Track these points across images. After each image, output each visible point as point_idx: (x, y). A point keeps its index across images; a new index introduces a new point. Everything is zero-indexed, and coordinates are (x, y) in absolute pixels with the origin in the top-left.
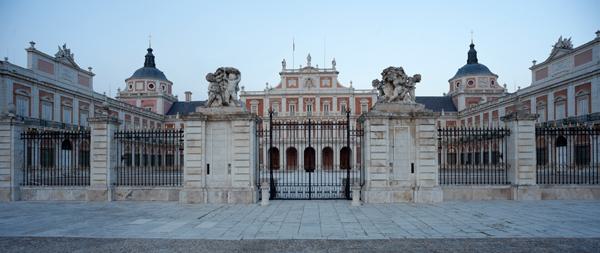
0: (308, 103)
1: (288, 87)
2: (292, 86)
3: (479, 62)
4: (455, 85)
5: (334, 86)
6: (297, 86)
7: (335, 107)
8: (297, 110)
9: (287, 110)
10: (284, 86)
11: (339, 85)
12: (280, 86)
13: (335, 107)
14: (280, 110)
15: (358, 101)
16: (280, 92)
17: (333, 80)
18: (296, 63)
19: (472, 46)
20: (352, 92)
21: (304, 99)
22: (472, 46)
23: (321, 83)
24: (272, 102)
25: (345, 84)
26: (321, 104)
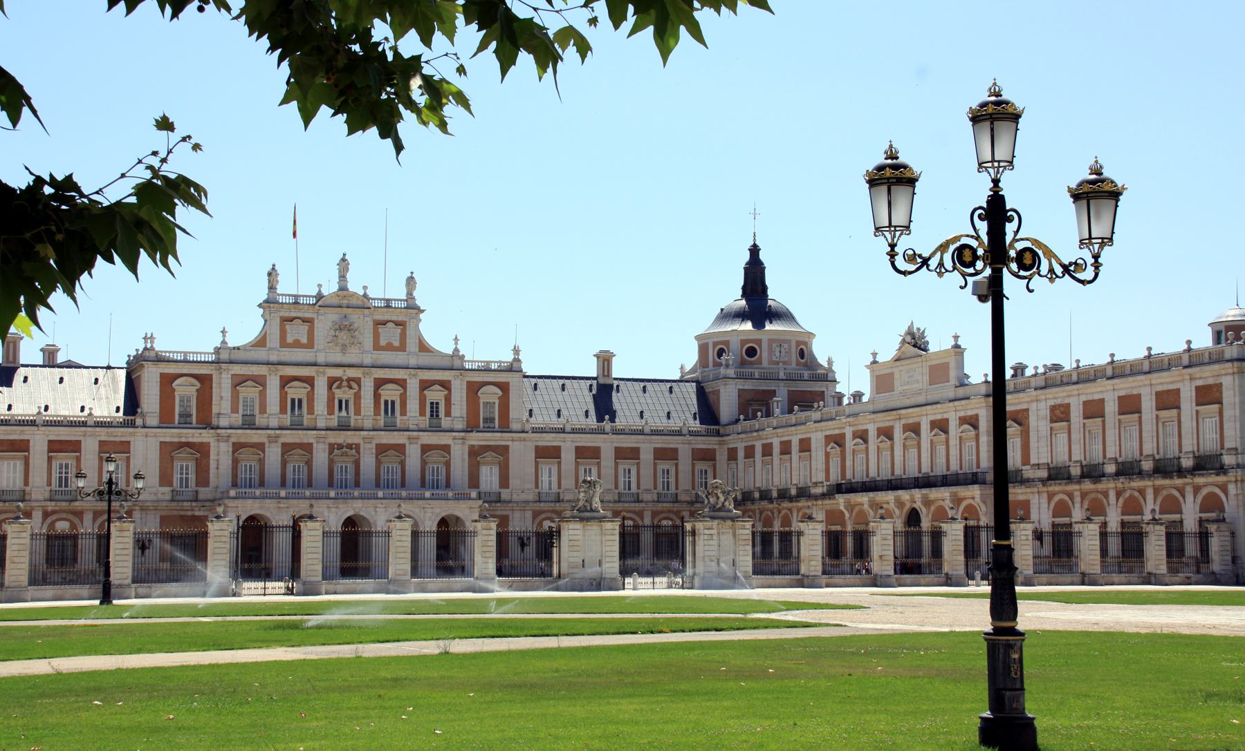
0: (339, 394)
1: (284, 344)
2: (297, 344)
3: (771, 293)
4: (712, 354)
5: (412, 346)
6: (310, 345)
7: (413, 405)
8: (311, 410)
9: (283, 410)
10: (273, 340)
11: (424, 347)
12: (261, 342)
13: (413, 405)
14: (263, 410)
15: (474, 389)
16: (261, 354)
17: (410, 332)
18: (308, 278)
19: (755, 250)
20: (457, 363)
21: (332, 382)
22: (755, 250)
23: (376, 337)
24: (239, 381)
25: (440, 342)
26: (377, 396)
